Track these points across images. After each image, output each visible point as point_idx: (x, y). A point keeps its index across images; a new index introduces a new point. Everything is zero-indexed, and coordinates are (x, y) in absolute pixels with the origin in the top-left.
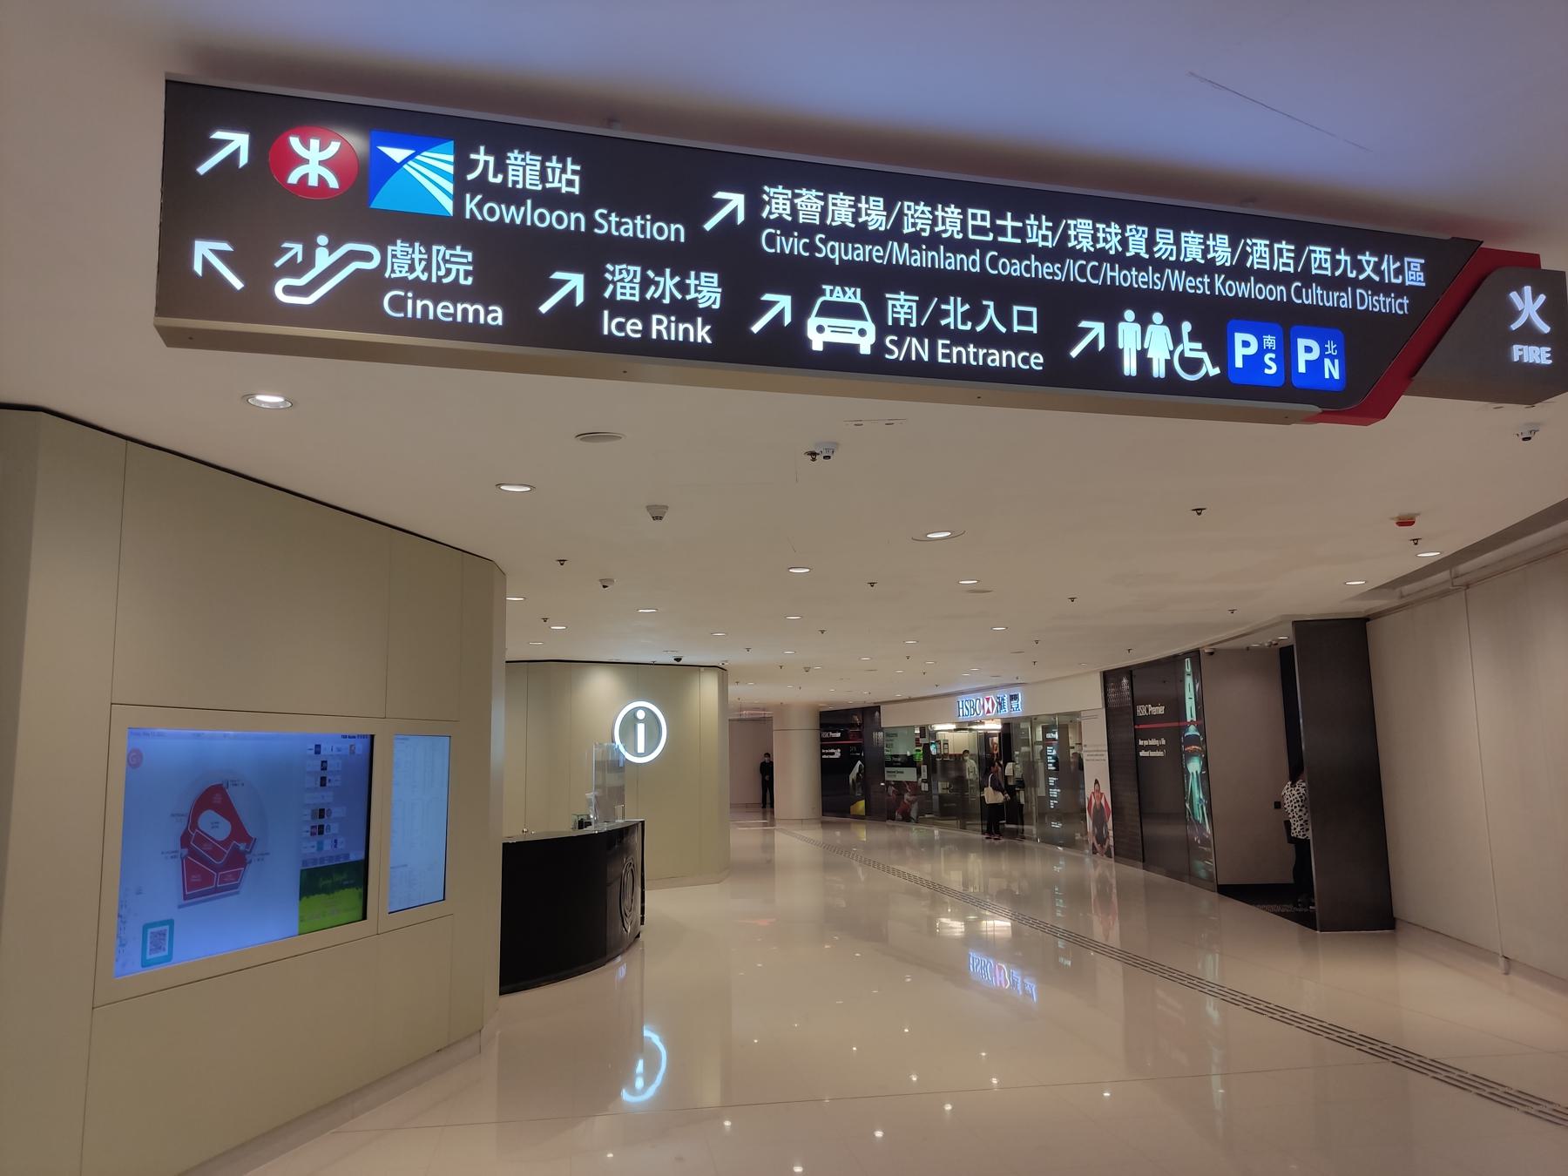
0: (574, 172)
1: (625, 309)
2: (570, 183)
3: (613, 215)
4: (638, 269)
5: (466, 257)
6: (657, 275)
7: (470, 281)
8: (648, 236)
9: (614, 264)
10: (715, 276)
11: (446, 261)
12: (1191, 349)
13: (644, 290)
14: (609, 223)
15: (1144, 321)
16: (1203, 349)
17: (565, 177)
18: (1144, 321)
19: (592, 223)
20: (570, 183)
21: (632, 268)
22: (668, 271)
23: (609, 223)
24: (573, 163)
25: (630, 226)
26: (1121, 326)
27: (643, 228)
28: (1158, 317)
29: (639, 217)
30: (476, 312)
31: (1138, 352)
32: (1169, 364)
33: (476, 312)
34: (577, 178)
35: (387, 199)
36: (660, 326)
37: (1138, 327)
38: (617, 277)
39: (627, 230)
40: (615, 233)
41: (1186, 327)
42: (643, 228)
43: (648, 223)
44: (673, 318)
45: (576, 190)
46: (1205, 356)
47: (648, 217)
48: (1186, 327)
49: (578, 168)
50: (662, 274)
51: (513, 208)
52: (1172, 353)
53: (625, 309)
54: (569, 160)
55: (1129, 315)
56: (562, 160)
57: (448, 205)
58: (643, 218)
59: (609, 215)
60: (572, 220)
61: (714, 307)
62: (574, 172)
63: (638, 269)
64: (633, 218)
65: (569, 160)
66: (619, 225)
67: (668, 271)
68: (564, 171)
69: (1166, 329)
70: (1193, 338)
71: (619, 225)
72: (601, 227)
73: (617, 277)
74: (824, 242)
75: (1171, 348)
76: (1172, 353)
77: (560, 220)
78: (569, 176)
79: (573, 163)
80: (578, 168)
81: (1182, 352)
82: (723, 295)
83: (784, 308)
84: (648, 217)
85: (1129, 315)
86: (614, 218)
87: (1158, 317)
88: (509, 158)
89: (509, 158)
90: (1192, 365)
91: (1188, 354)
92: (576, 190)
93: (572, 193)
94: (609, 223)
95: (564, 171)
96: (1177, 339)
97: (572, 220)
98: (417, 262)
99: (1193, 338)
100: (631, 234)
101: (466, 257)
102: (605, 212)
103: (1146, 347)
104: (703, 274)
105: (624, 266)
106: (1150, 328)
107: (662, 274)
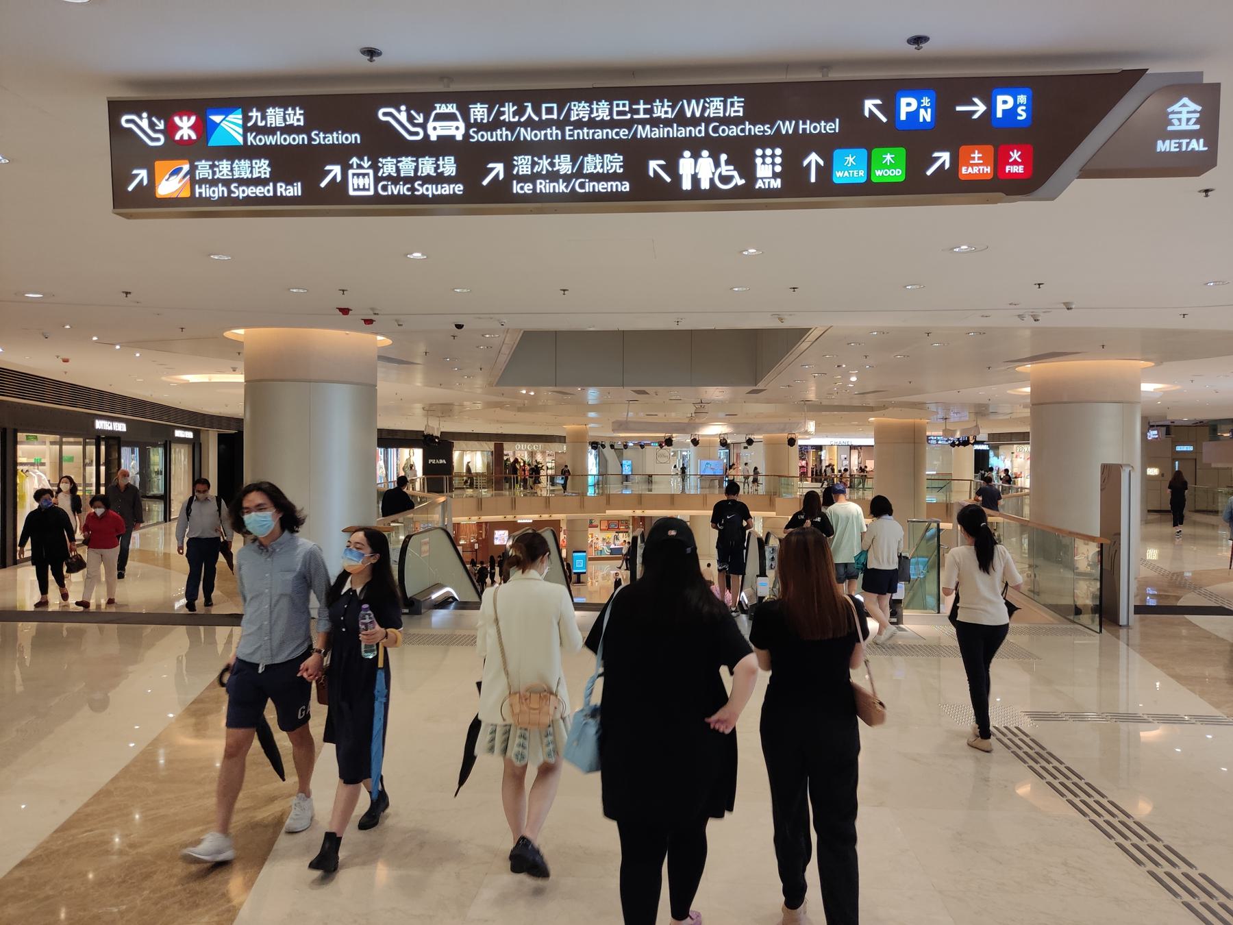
0: (300, 114)
1: (523, 179)
2: (298, 120)
3: (321, 133)
4: (530, 157)
5: (619, 158)
6: (539, 159)
7: (622, 170)
8: (340, 142)
9: (518, 155)
10: (569, 156)
11: (611, 162)
12: (726, 170)
13: (533, 168)
14: (319, 138)
15: (696, 156)
16: (735, 170)
17: (296, 117)
18: (696, 156)
19: (310, 139)
20: (298, 120)
21: (526, 157)
22: (544, 156)
23: (319, 138)
24: (668, 101)
25: (331, 138)
26: (682, 161)
27: (338, 138)
28: (705, 153)
29: (335, 133)
30: (617, 186)
31: (692, 175)
32: (712, 180)
33: (617, 186)
34: (302, 118)
35: (215, 141)
36: (543, 186)
37: (692, 160)
38: (520, 163)
39: (329, 141)
40: (322, 143)
41: (724, 157)
42: (338, 138)
43: (340, 136)
44: (548, 181)
45: (302, 123)
46: (735, 174)
47: (340, 132)
48: (724, 157)
49: (302, 112)
50: (541, 158)
51: (271, 137)
52: (713, 174)
53: (523, 179)
54: (297, 108)
55: (687, 154)
56: (294, 109)
57: (241, 140)
58: (337, 133)
59: (319, 134)
60: (300, 139)
61: (568, 173)
62: (300, 114)
63: (530, 157)
64: (332, 133)
65: (297, 108)
66: (324, 138)
67: (544, 156)
68: (295, 114)
69: (711, 160)
70: (728, 163)
71: (324, 138)
72: (315, 140)
73: (520, 163)
74: (476, 133)
75: (714, 171)
76: (713, 174)
77: (294, 139)
78: (298, 116)
79: (668, 101)
80: (302, 112)
81: (720, 173)
82: (456, 167)
83: (499, 171)
84: (340, 132)
85: (687, 154)
86: (322, 135)
87: (705, 153)
88: (267, 112)
89: (267, 112)
90: (725, 179)
91: (724, 173)
92: (302, 123)
93: (300, 125)
94: (319, 138)
95: (295, 114)
96: (717, 164)
97: (300, 139)
98: (597, 164)
99: (728, 163)
100: (331, 142)
101: (619, 158)
102: (317, 132)
103: (697, 171)
104: (562, 156)
105: (523, 157)
106: (700, 160)
107: (541, 158)
